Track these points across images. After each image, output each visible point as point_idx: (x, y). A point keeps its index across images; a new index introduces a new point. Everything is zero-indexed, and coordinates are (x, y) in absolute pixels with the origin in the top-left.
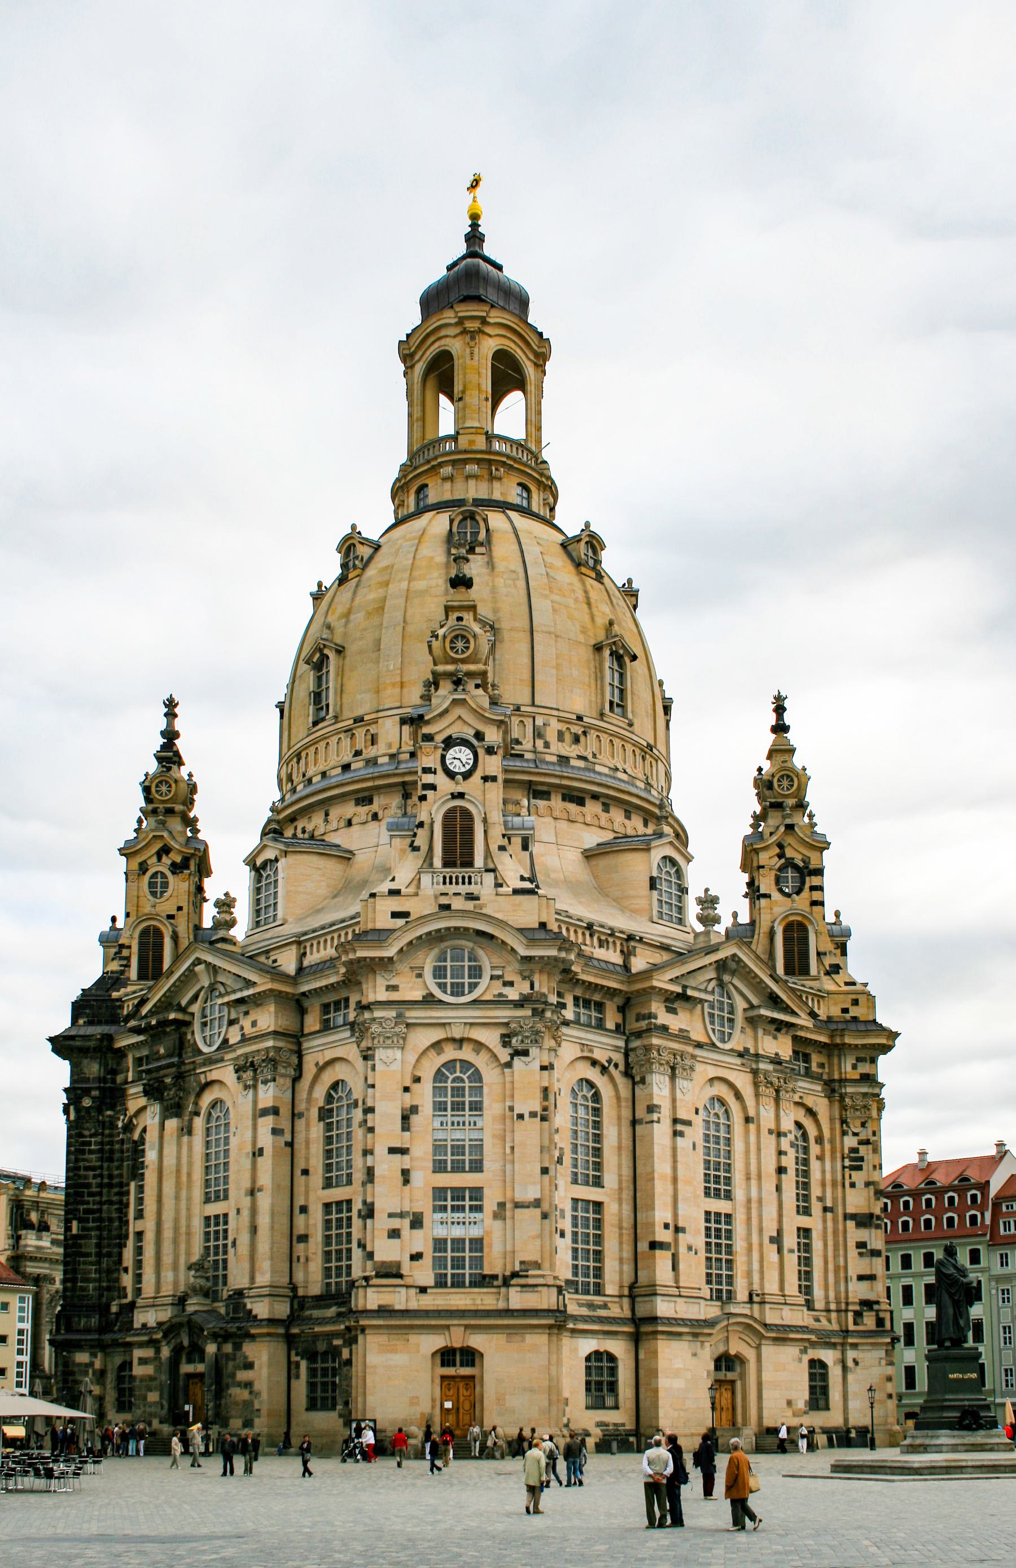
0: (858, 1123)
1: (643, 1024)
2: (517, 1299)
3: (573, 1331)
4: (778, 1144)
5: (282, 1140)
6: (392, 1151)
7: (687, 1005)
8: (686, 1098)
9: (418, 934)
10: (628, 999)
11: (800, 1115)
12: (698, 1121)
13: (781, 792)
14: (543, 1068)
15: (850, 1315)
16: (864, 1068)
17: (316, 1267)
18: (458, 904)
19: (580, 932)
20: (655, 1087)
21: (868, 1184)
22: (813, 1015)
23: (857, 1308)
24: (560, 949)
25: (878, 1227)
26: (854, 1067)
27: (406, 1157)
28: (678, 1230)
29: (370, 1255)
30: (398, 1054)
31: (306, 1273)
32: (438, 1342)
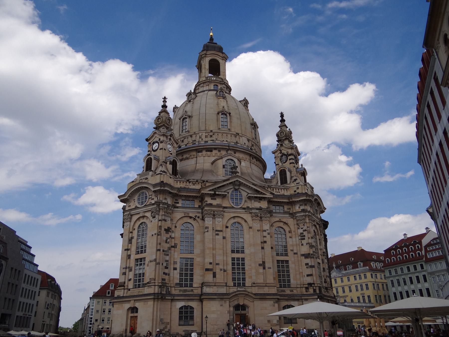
0: (302, 224)
2: (147, 290)
3: (172, 300)
8: (220, 223)
10: (202, 198)
11: (281, 225)
13: (284, 136)
14: (160, 220)
15: (304, 288)
16: (302, 208)
21: (307, 244)
22: (271, 193)
23: (307, 286)
24: (161, 187)
25: (311, 258)
26: (299, 208)
27: (129, 251)
30: (129, 223)
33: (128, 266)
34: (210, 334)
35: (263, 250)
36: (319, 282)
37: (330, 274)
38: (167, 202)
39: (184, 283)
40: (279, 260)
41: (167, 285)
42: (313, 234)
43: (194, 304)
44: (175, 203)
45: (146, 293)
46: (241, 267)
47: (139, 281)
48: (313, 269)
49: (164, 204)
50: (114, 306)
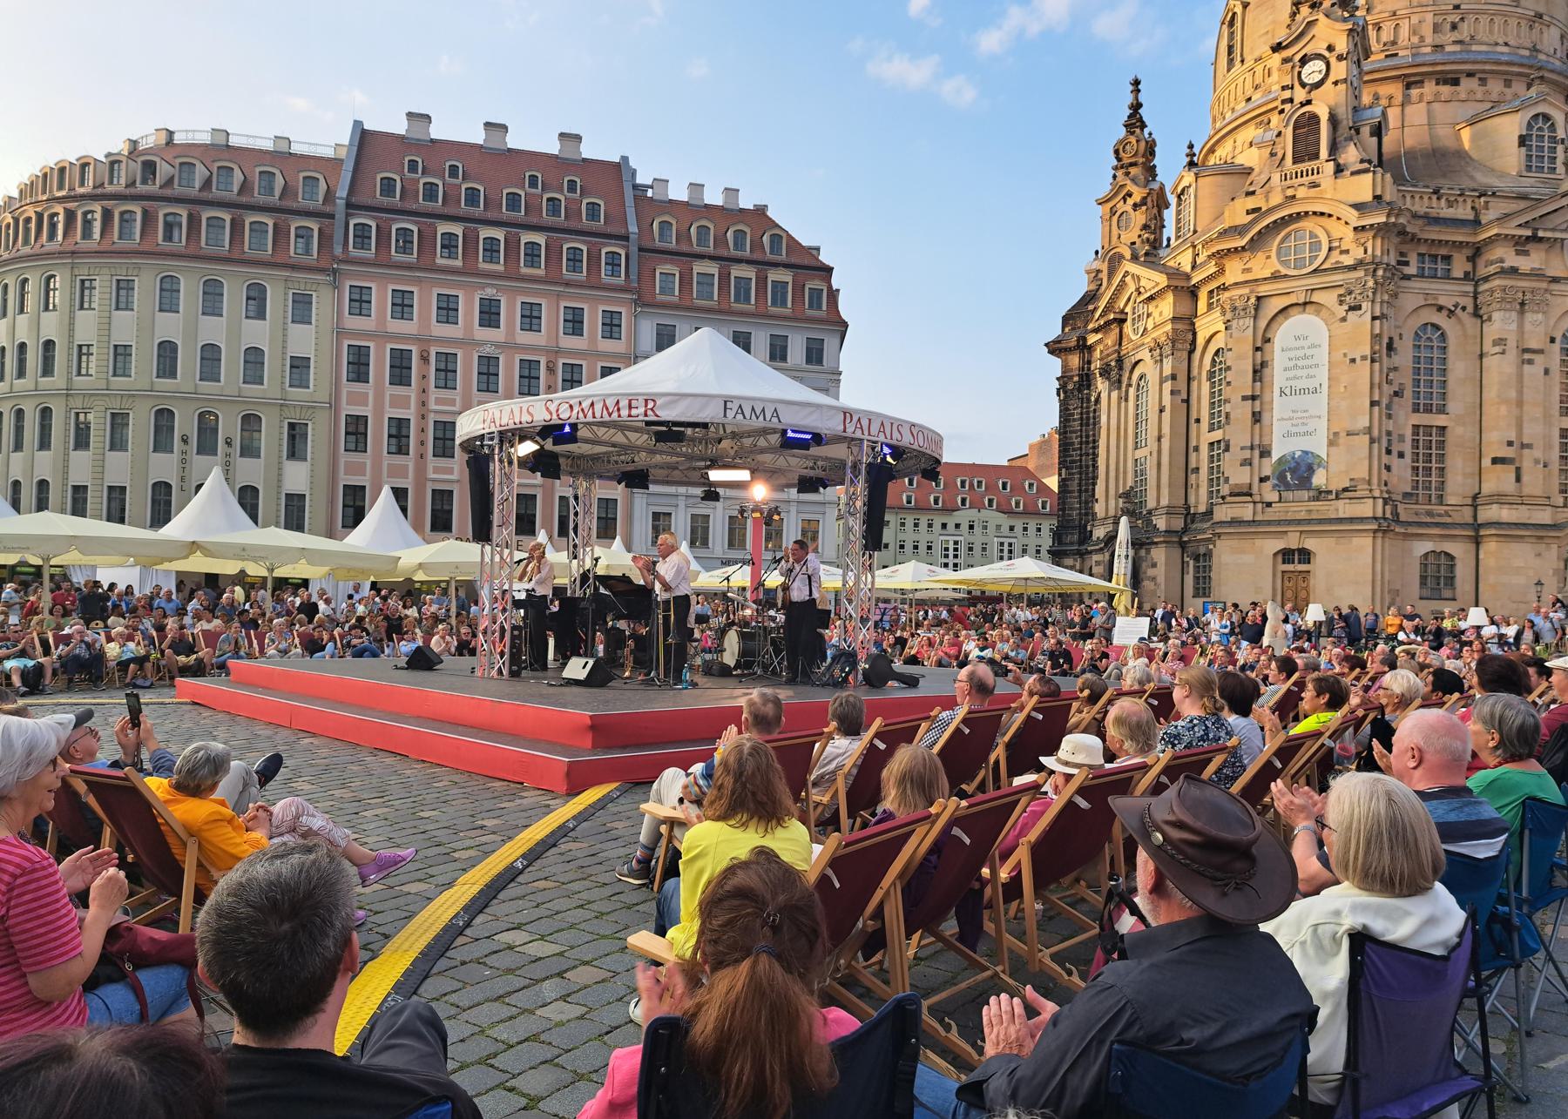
1: (1492, 269)
2: (1344, 509)
3: (1406, 536)
5: (1179, 399)
6: (1244, 398)
7: (1544, 246)
9: (1265, 223)
10: (1478, 249)
12: (1557, 346)
17: (1203, 491)
18: (1301, 193)
19: (1426, 198)
24: (1388, 216)
27: (1257, 403)
28: (1523, 446)
29: (1227, 480)
31: (1197, 495)
32: (1280, 545)
33: (1257, 442)
41: (1394, 497)
43: (1459, 550)
44: (1399, 263)
45: (1341, 515)
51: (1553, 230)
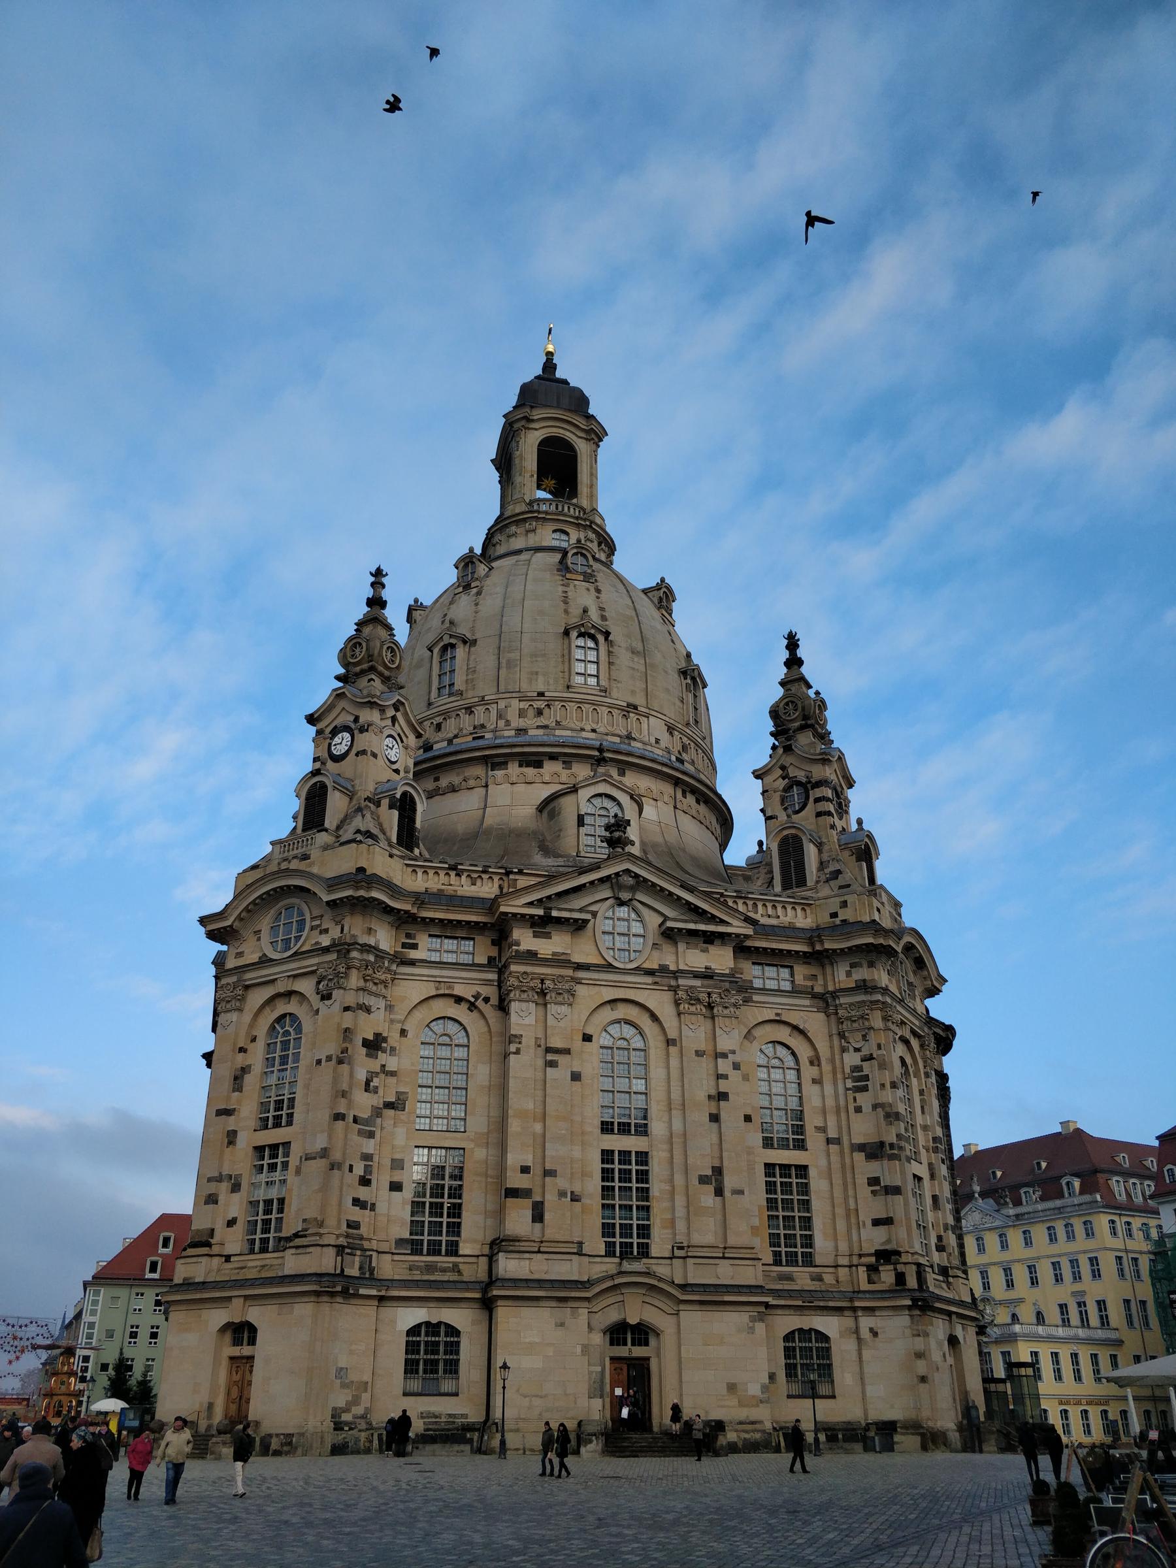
4: (716, 1067)
8: (562, 1024)
20: (514, 1017)
24: (357, 888)
25: (892, 1157)
34: (517, 1430)
35: (715, 1125)
36: (917, 1248)
37: (958, 1219)
38: (377, 941)
39: (426, 1238)
40: (774, 1165)
42: (898, 1069)
46: (634, 1185)
47: (268, 1228)
48: (899, 1199)
49: (366, 948)
50: (172, 1316)
51: (571, 910)
